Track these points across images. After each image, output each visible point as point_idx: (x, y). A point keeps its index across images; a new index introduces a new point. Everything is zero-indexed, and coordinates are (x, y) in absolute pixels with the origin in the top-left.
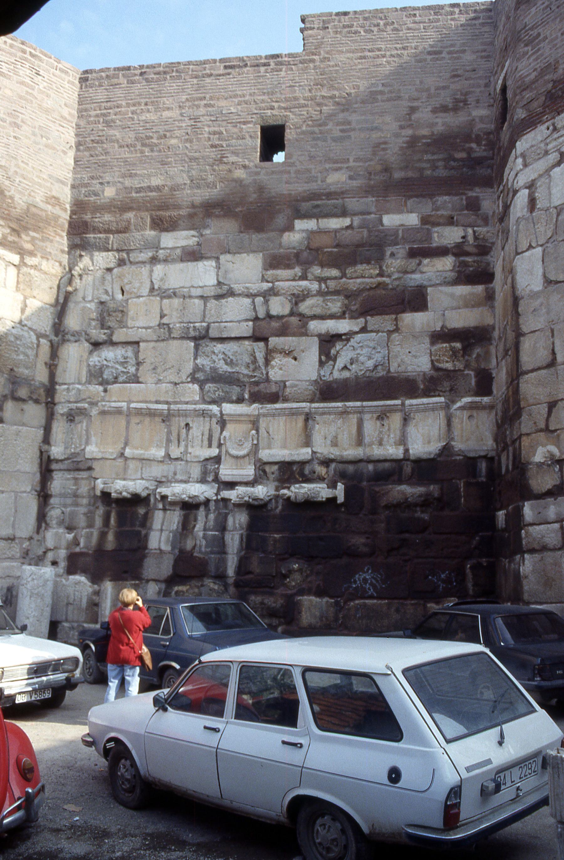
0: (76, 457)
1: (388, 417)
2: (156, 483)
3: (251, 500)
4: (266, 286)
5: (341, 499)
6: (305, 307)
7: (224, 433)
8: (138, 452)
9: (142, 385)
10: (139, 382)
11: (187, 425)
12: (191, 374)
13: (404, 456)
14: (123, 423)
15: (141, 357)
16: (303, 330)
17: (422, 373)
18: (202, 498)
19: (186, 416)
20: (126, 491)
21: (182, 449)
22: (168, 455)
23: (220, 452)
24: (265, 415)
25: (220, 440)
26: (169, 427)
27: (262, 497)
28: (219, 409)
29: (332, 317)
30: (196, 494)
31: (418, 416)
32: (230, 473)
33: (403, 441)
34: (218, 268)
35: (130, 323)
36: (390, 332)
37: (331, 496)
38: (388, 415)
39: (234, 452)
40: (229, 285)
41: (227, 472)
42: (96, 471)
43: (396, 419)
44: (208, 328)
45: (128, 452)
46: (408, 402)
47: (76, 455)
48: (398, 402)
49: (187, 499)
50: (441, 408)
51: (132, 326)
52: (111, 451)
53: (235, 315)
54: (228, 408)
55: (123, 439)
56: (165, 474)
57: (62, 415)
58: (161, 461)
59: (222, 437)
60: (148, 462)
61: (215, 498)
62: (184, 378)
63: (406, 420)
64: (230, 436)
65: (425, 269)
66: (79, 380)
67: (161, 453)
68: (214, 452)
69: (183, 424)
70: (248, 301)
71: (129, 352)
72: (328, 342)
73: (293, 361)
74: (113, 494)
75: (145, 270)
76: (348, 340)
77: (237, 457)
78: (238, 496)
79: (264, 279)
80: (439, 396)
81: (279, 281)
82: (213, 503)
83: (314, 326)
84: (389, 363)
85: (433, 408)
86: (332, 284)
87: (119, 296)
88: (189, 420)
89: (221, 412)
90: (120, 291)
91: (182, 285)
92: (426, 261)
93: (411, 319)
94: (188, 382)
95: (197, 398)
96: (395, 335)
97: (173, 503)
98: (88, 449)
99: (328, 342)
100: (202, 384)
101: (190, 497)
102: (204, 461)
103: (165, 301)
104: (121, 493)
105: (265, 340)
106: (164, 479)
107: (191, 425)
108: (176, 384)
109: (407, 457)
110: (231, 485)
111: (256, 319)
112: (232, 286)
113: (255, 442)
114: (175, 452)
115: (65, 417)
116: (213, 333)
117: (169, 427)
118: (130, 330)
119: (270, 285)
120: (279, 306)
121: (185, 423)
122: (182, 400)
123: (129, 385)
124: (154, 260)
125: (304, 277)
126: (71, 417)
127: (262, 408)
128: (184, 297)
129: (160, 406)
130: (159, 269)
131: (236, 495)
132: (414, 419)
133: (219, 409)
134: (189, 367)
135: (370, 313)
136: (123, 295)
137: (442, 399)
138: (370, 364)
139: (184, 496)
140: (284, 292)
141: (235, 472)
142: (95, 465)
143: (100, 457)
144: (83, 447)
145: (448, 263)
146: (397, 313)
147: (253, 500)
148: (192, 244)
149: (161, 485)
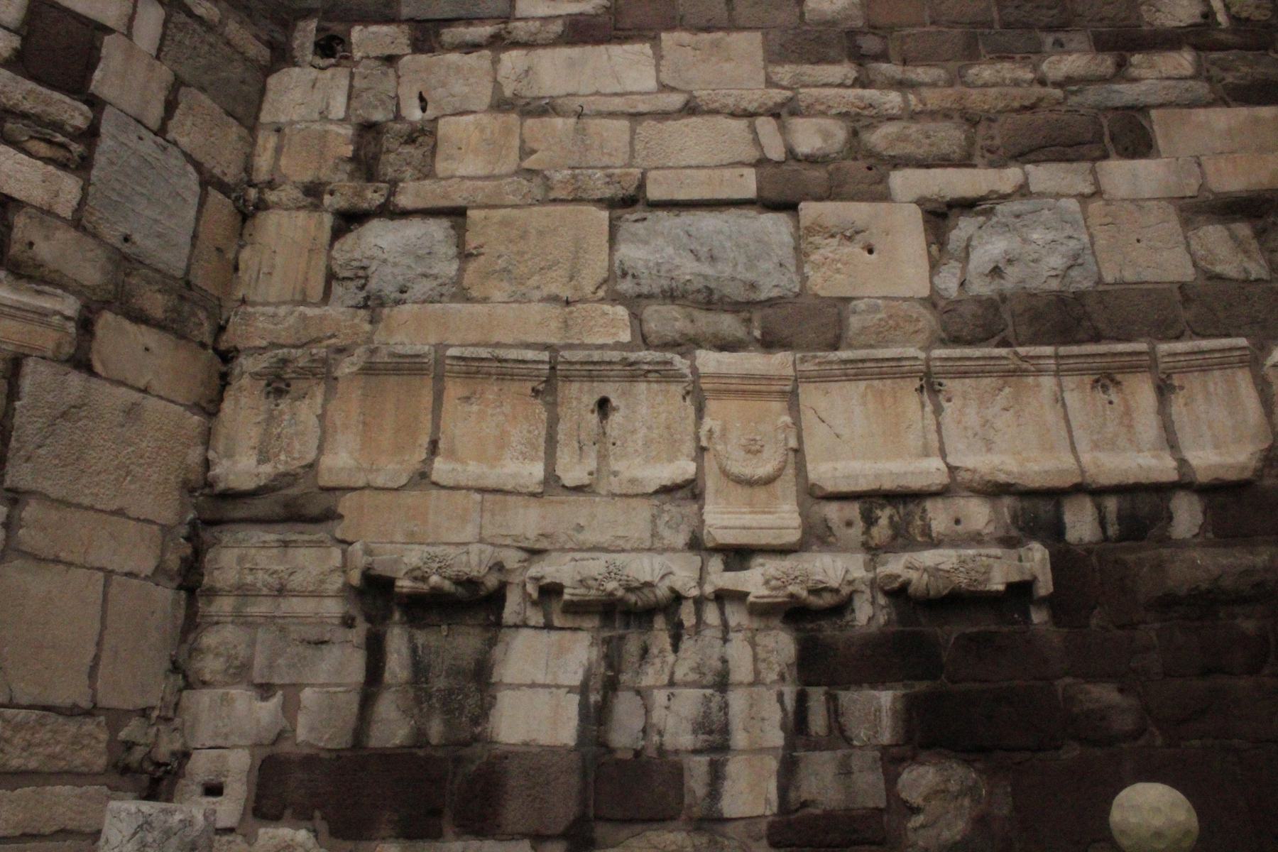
0: (289, 485)
1: (1118, 383)
2: (523, 555)
3: (804, 594)
4: (778, 95)
5: (1045, 586)
6: (879, 138)
7: (708, 423)
8: (472, 471)
9: (478, 308)
10: (469, 300)
11: (603, 406)
12: (605, 281)
13: (1182, 475)
14: (427, 398)
15: (472, 241)
16: (880, 188)
17: (1175, 288)
18: (662, 592)
19: (601, 378)
20: (439, 571)
21: (591, 463)
22: (551, 481)
23: (700, 469)
24: (809, 379)
25: (698, 439)
26: (552, 407)
27: (834, 583)
28: (688, 362)
29: (945, 162)
30: (648, 579)
31: (1194, 382)
32: (738, 523)
33: (1170, 440)
34: (658, 57)
35: (441, 166)
36: (1083, 198)
37: (1015, 578)
38: (1119, 377)
39: (736, 468)
40: (690, 92)
41: (725, 518)
42: (346, 522)
43: (1142, 392)
44: (642, 186)
45: (442, 469)
46: (1164, 347)
47: (288, 478)
48: (1141, 346)
49: (620, 593)
50: (1242, 362)
51: (449, 173)
52: (392, 470)
53: (701, 156)
54: (709, 360)
55: (425, 440)
56: (549, 530)
57: (256, 376)
58: (533, 495)
59: (703, 432)
60: (499, 497)
61: (695, 592)
62: (588, 289)
63: (1164, 390)
64: (724, 430)
65: (1135, 72)
66: (304, 292)
67: (537, 470)
68: (684, 468)
69: (591, 400)
70: (742, 124)
71: (438, 229)
72: (939, 216)
73: (866, 254)
74: (399, 583)
75: (479, 60)
76: (989, 212)
77: (750, 483)
78: (767, 582)
79: (770, 83)
80: (1238, 335)
81: (807, 86)
82: (690, 602)
83: (905, 182)
84: (1097, 262)
85: (1224, 362)
86: (934, 98)
87: (415, 114)
88: (610, 390)
89: (694, 370)
90: (416, 102)
91: (571, 90)
92: (1136, 58)
93: (1121, 174)
94: (602, 300)
95: (625, 337)
96: (1095, 206)
97: (577, 609)
98: (327, 461)
99: (939, 216)
100: (635, 302)
101: (629, 589)
102: (656, 492)
103: (530, 122)
104: (424, 579)
105: (789, 207)
106: (544, 544)
107: (614, 402)
108: (568, 303)
109: (1187, 480)
110: (738, 556)
111: (761, 163)
112: (695, 93)
113: (793, 443)
114: (573, 473)
115: (263, 383)
116: (654, 193)
117: (552, 407)
118: (443, 183)
119: (789, 94)
120: (809, 136)
121: (596, 397)
122: (588, 341)
123: (438, 306)
124: (498, 43)
125: (860, 83)
126: (277, 385)
127: (803, 360)
128: (580, 115)
129: (530, 355)
130: (512, 60)
131: (760, 580)
132: (1182, 388)
133: (688, 362)
134: (596, 266)
135: (1032, 157)
136: (424, 110)
137: (1242, 342)
138: (1056, 261)
139: (611, 586)
140: (822, 108)
141: (748, 519)
142: (346, 504)
143: (361, 483)
144: (310, 457)
145: (1186, 64)
146: (1094, 160)
147: (815, 592)
148: (592, 11)
149: (536, 558)
